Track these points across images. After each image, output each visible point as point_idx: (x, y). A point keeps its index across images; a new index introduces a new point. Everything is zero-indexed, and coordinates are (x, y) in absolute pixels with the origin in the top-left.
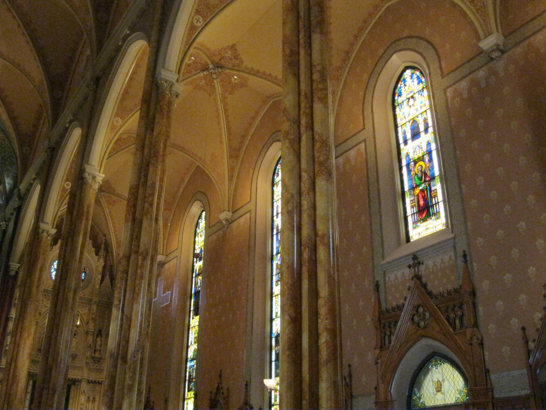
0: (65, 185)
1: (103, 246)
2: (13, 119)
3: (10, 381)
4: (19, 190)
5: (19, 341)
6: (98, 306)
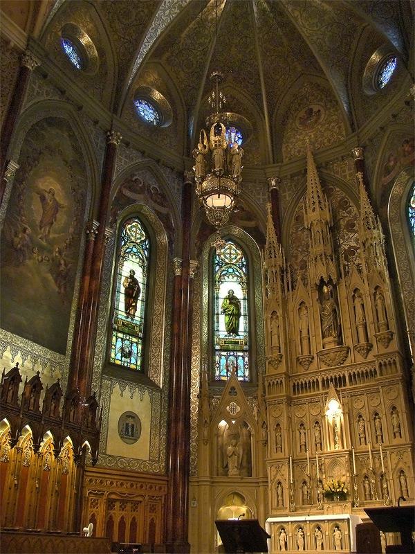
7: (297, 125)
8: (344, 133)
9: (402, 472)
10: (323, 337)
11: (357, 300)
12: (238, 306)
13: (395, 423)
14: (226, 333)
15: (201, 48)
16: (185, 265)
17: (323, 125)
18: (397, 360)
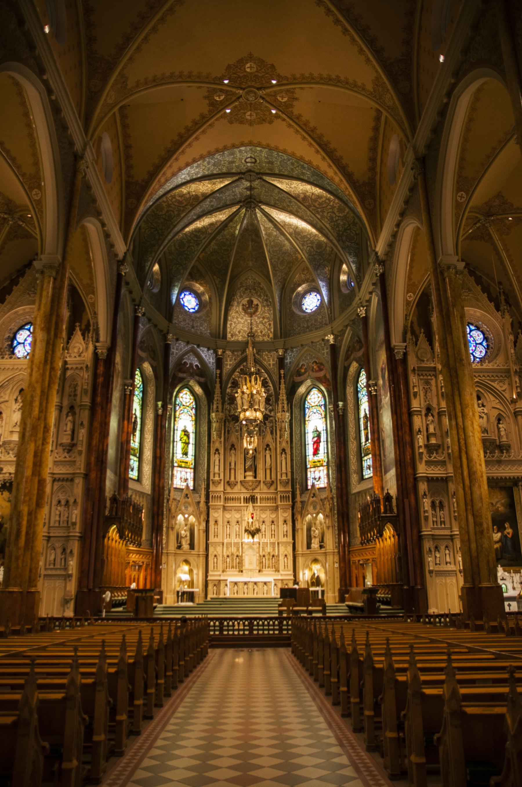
0: (459, 199)
1: (503, 298)
2: (343, 169)
3: (467, 482)
4: (376, 253)
5: (463, 424)
7: (241, 309)
8: (272, 330)
9: (286, 556)
10: (245, 471)
11: (267, 452)
12: (188, 436)
13: (285, 530)
14: (181, 455)
15: (196, 239)
16: (164, 407)
17: (259, 318)
18: (290, 496)
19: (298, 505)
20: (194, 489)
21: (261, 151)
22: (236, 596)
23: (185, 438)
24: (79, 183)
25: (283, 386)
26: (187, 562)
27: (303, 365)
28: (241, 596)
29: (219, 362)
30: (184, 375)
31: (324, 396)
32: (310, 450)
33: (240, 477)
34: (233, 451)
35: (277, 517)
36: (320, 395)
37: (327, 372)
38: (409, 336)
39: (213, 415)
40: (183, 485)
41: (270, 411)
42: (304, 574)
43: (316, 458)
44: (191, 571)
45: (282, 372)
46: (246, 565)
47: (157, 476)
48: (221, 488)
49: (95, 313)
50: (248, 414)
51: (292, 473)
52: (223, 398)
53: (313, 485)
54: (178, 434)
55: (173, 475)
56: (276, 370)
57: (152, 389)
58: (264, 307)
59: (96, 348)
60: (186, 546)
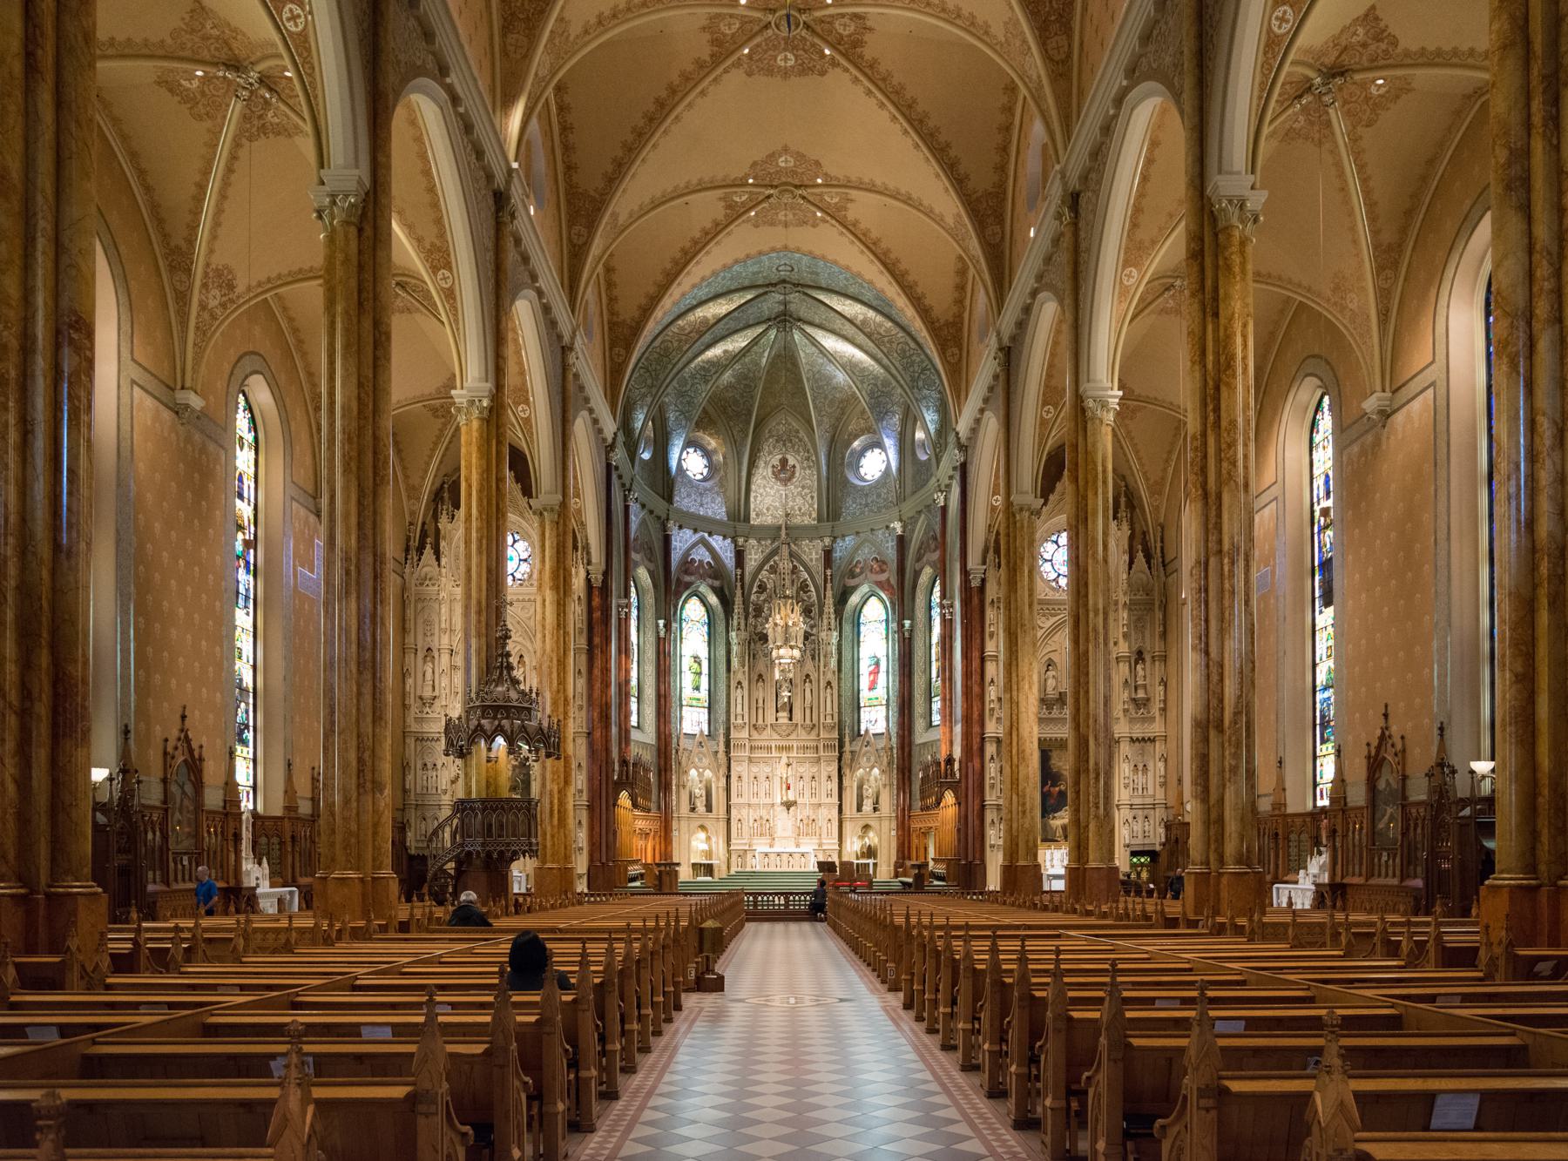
0: (1044, 414)
6: (1130, 610)
12: (700, 664)
16: (667, 626)
19: (847, 756)
20: (709, 735)
21: (801, 259)
22: (766, 869)
23: (696, 665)
24: (571, 387)
25: (829, 593)
26: (702, 827)
27: (858, 562)
28: (772, 869)
29: (740, 556)
30: (693, 578)
31: (886, 607)
32: (864, 682)
33: (770, 719)
34: (760, 684)
35: (819, 771)
36: (881, 607)
37: (890, 575)
38: (991, 555)
39: (733, 634)
40: (696, 730)
41: (812, 627)
42: (852, 843)
43: (873, 694)
44: (708, 838)
45: (829, 572)
46: (779, 832)
47: (662, 720)
48: (745, 734)
49: (583, 525)
50: (782, 652)
51: (840, 713)
52: (746, 610)
53: (867, 731)
54: (687, 662)
55: (681, 718)
56: (821, 568)
57: (650, 600)
58: (804, 469)
59: (588, 573)
60: (701, 808)
